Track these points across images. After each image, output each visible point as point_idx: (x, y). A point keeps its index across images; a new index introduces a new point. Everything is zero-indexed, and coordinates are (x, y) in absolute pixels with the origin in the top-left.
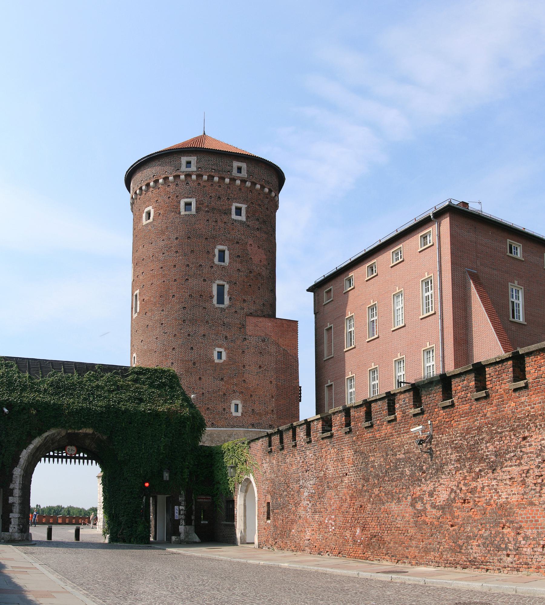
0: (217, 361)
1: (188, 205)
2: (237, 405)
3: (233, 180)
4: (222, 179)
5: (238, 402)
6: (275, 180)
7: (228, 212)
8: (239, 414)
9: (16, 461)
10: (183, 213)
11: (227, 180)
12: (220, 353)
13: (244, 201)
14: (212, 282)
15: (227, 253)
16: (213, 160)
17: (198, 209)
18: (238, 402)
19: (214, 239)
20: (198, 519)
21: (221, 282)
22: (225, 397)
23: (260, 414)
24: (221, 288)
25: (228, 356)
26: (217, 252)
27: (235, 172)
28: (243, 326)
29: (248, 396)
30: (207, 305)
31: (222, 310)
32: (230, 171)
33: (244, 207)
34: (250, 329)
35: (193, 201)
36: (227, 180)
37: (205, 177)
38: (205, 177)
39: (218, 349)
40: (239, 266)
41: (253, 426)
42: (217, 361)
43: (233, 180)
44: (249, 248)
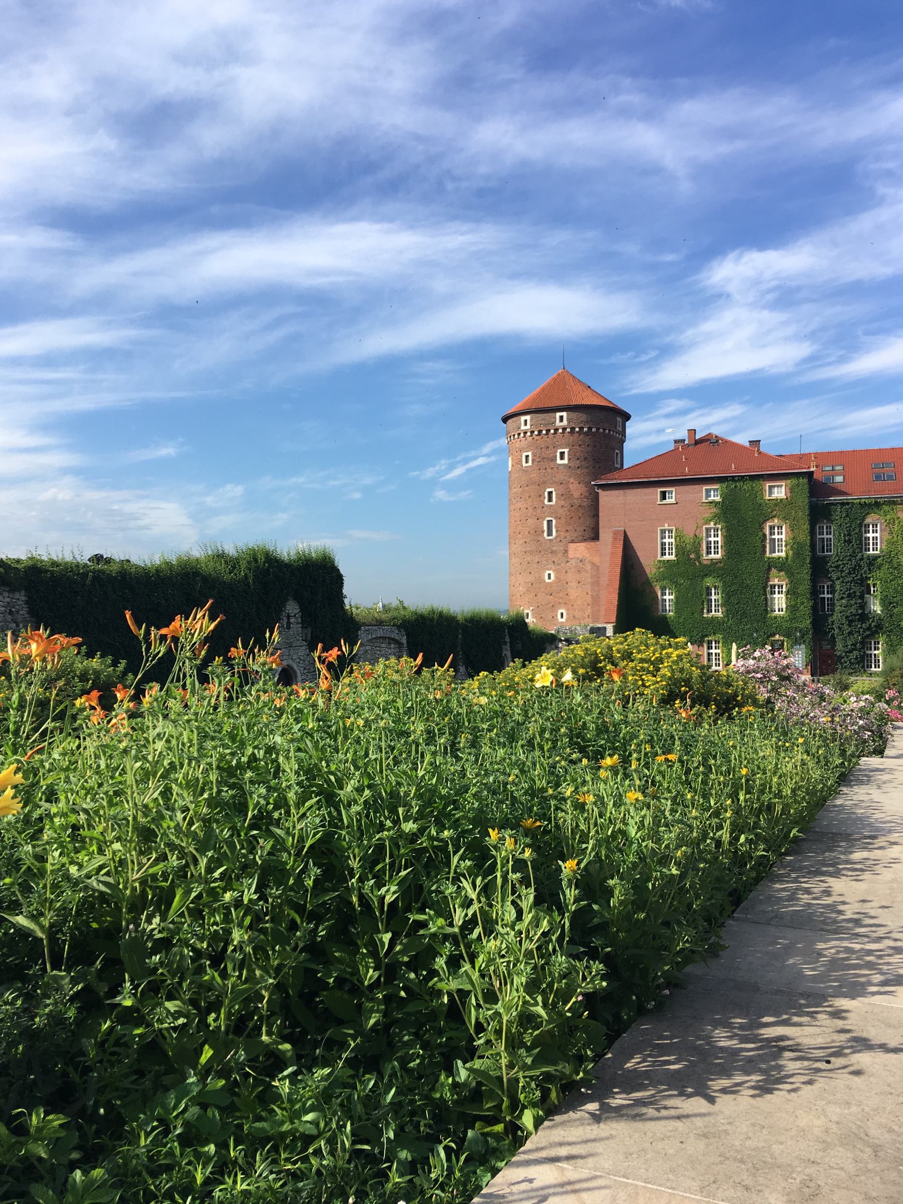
0: (547, 581)
1: (527, 456)
4: (548, 431)
8: (564, 620)
10: (524, 465)
12: (549, 575)
15: (554, 494)
17: (533, 460)
18: (563, 611)
21: (550, 519)
22: (554, 608)
24: (550, 522)
25: (556, 577)
26: (546, 494)
27: (558, 423)
28: (566, 551)
30: (540, 538)
31: (550, 540)
32: (554, 423)
33: (566, 451)
34: (571, 554)
35: (530, 454)
39: (548, 572)
40: (563, 503)
43: (556, 430)
44: (571, 486)
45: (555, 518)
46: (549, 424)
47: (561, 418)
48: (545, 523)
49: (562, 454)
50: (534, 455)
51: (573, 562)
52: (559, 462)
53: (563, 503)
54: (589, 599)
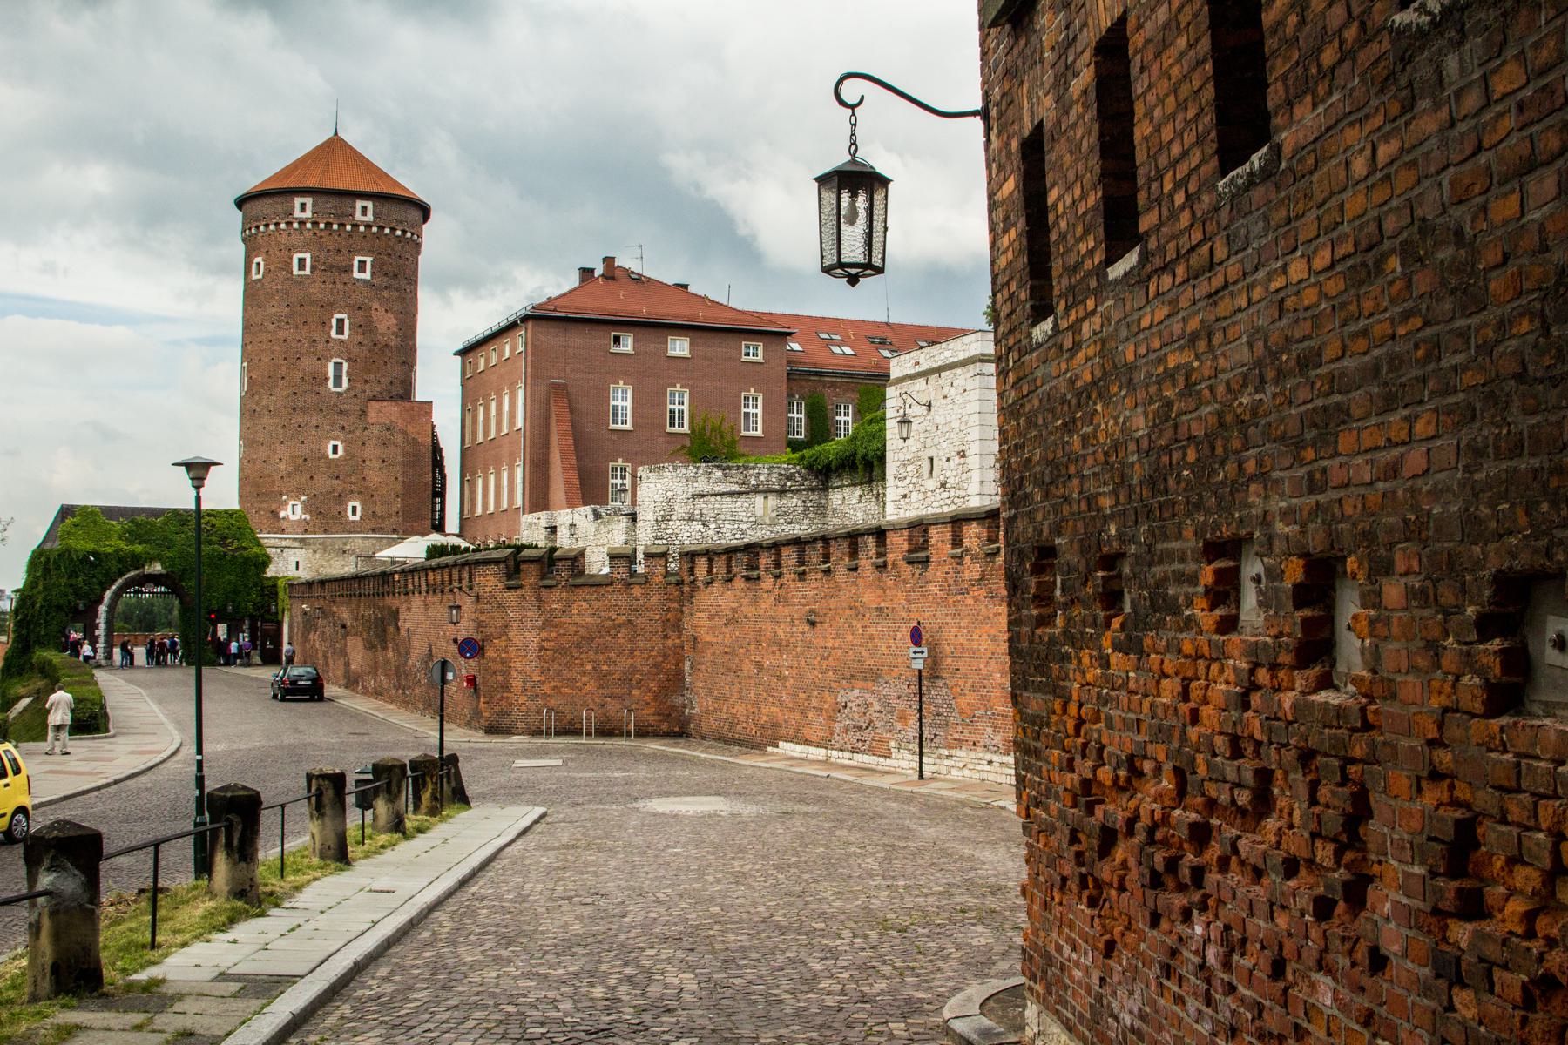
0: (331, 456)
1: (302, 261)
2: (354, 508)
3: (355, 226)
4: (342, 225)
5: (357, 504)
6: (415, 215)
7: (349, 269)
8: (357, 518)
9: (100, 601)
10: (296, 271)
11: (349, 228)
12: (335, 448)
13: (369, 253)
14: (328, 360)
15: (347, 323)
16: (332, 202)
17: (313, 268)
19: (330, 307)
20: (264, 644)
22: (341, 498)
23: (382, 517)
24: (338, 366)
25: (345, 450)
26: (334, 322)
27: (358, 217)
28: (364, 413)
29: (367, 495)
31: (339, 394)
32: (353, 215)
33: (369, 260)
34: (372, 415)
35: (308, 256)
36: (349, 228)
37: (322, 226)
38: (322, 226)
39: (333, 442)
40: (360, 338)
41: (373, 531)
42: (331, 456)
45: (348, 360)
46: (343, 215)
47: (364, 209)
48: (331, 367)
49: (362, 265)
50: (315, 259)
51: (375, 430)
52: (356, 275)
53: (360, 338)
54: (398, 487)
